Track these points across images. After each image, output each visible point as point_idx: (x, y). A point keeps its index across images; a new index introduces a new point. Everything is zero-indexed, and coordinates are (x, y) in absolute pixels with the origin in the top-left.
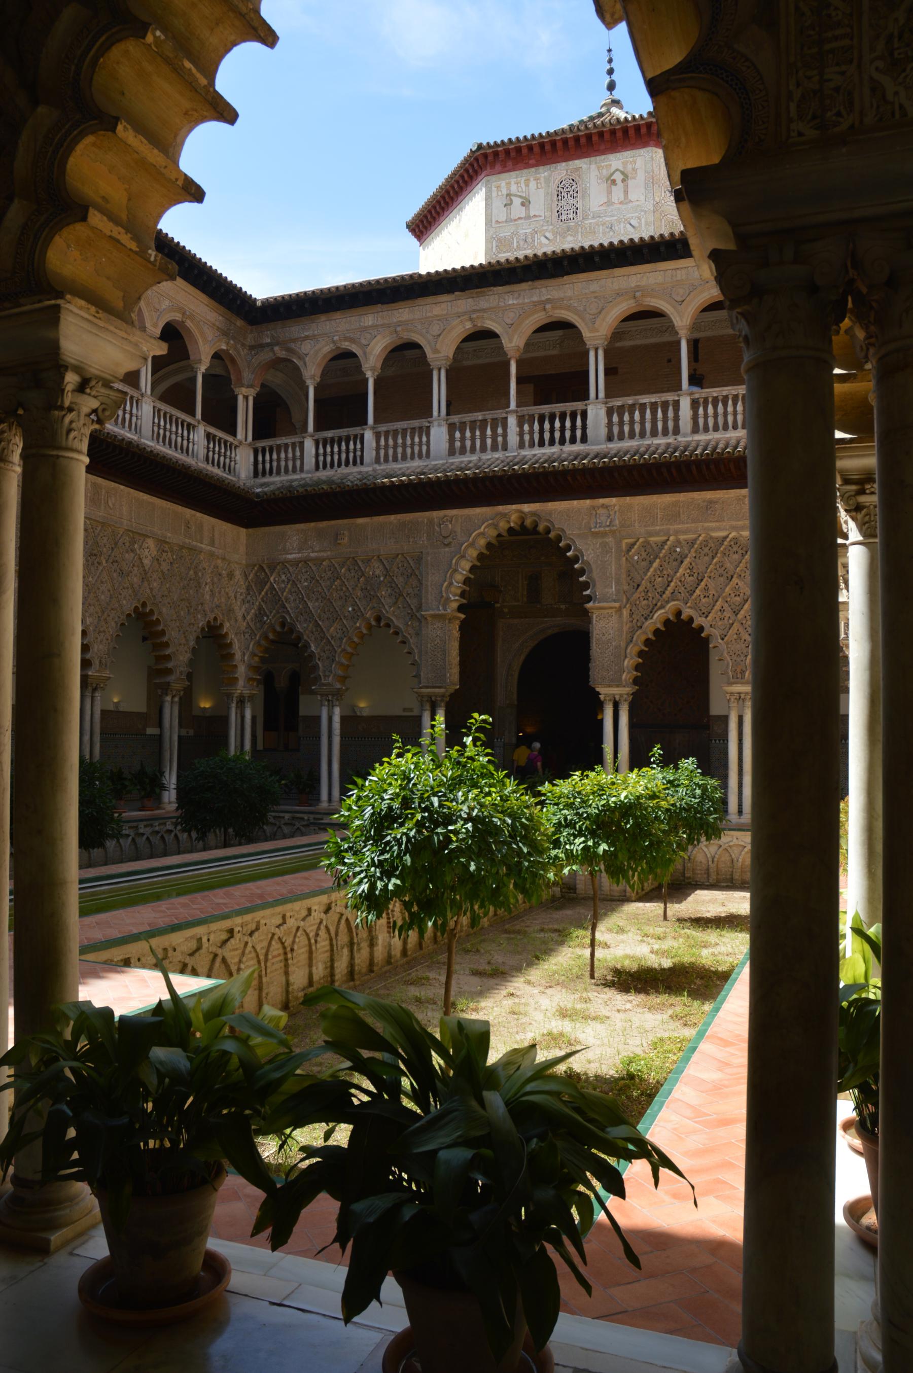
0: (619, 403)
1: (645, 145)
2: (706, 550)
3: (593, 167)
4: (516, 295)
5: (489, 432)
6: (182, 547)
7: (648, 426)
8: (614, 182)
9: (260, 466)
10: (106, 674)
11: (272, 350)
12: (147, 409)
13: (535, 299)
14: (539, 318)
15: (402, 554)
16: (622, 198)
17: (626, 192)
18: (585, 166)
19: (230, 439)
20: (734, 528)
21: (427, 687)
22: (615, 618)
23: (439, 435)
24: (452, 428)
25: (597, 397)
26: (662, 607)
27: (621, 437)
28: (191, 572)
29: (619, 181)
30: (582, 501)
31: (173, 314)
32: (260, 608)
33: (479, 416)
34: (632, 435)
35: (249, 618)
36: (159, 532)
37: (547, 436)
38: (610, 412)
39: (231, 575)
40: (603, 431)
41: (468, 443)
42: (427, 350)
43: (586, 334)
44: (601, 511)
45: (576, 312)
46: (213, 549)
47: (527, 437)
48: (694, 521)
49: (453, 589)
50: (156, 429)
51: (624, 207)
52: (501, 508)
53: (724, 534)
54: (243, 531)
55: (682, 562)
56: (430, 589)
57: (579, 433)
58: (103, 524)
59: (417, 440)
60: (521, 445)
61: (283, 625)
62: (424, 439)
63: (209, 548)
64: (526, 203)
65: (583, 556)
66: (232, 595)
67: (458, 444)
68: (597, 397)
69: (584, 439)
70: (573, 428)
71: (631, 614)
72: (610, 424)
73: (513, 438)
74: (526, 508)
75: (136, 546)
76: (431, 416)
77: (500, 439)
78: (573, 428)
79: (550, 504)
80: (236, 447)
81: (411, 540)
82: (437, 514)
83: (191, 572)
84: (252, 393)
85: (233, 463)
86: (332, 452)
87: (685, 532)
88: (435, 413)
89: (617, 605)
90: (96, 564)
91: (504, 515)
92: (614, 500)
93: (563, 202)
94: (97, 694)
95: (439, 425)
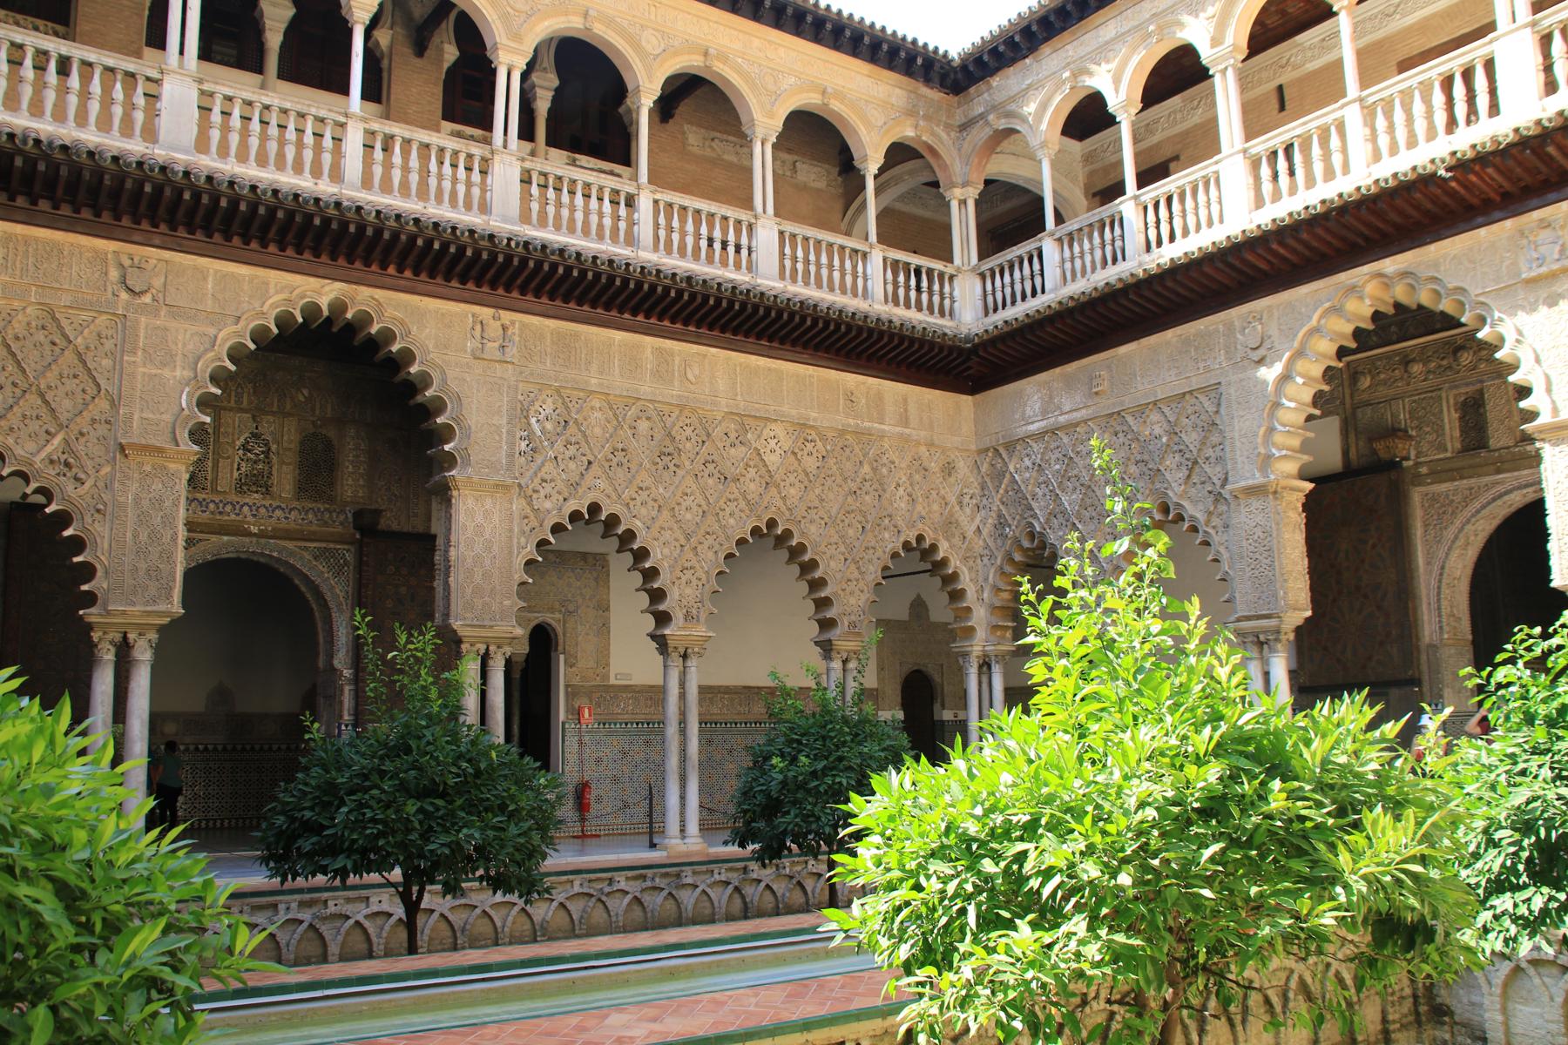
6: (842, 433)
9: (990, 299)
10: (700, 630)
11: (987, 123)
12: (767, 235)
15: (1191, 392)
19: (937, 265)
21: (1248, 618)
28: (866, 468)
31: (805, 95)
32: (1000, 516)
35: (985, 532)
36: (794, 412)
39: (949, 469)
46: (907, 431)
49: (1278, 438)
50: (788, 263)
54: (966, 400)
56: (1238, 444)
58: (682, 408)
61: (1032, 535)
63: (898, 429)
66: (953, 500)
75: (749, 436)
80: (951, 278)
82: (1235, 314)
83: (866, 468)
84: (972, 193)
85: (947, 302)
86: (1082, 253)
90: (672, 468)
91: (1352, 289)
94: (689, 663)
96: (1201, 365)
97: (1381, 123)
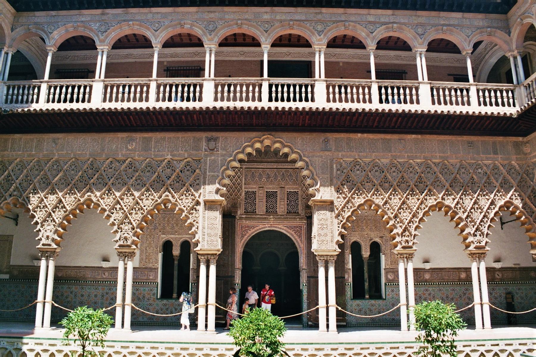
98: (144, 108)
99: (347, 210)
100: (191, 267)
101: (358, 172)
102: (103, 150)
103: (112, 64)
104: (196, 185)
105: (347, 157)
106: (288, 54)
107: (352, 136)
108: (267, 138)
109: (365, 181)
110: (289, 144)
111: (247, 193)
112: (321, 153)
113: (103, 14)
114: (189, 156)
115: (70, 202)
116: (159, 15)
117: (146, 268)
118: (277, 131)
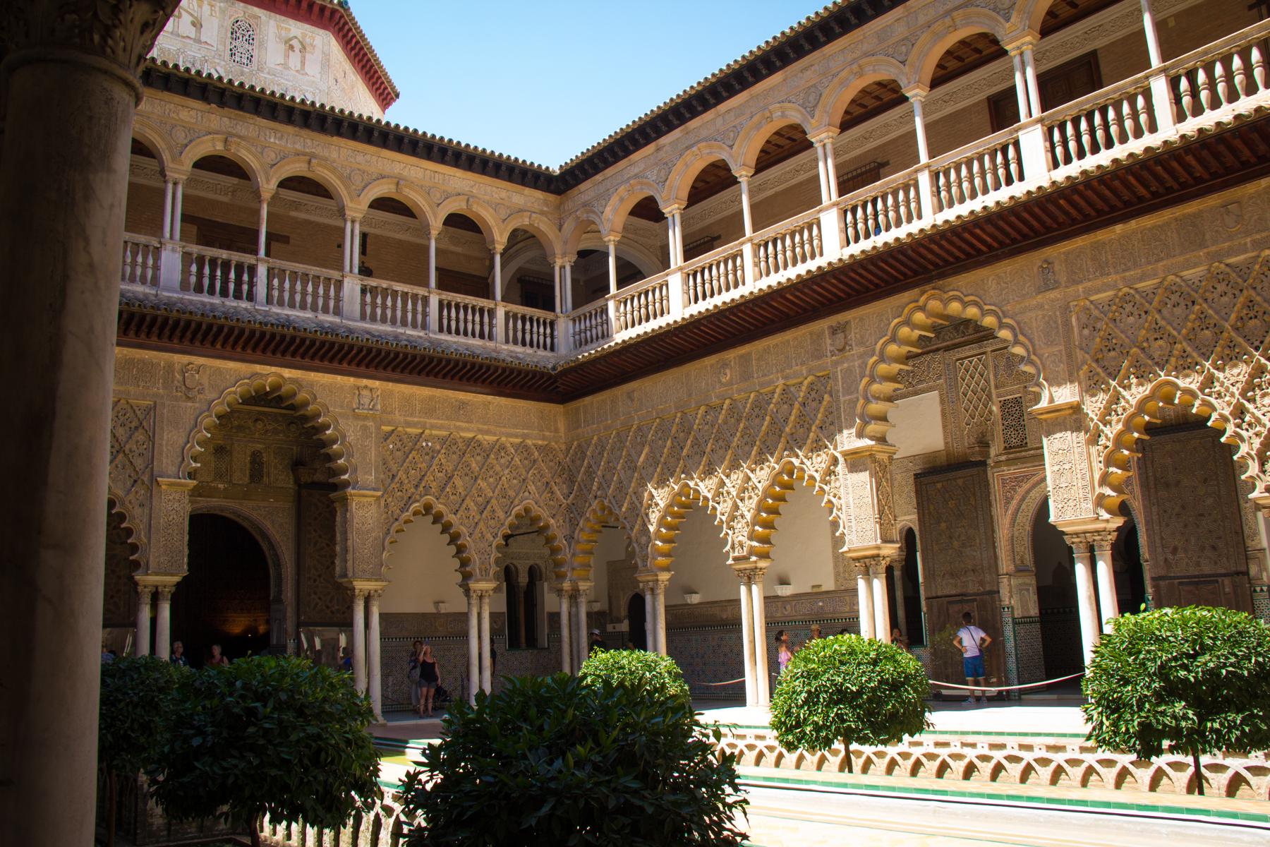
0: (374, 284)
1: (325, 27)
2: (454, 448)
3: (272, 22)
4: (279, 135)
5: (232, 275)
7: (399, 314)
8: (292, 47)
13: (299, 147)
14: (296, 168)
16: (299, 67)
17: (303, 63)
18: (263, 18)
20: (480, 431)
21: (157, 574)
22: (374, 509)
23: (171, 261)
24: (186, 257)
25: (351, 271)
26: (417, 501)
27: (373, 319)
29: (297, 50)
30: (346, 378)
33: (224, 254)
34: (384, 320)
37: (298, 298)
38: (364, 291)
40: (358, 308)
41: (206, 282)
42: (166, 156)
43: (347, 202)
44: (365, 392)
45: (341, 177)
47: (276, 293)
48: (448, 418)
51: (300, 77)
52: (258, 368)
53: (470, 435)
55: (433, 457)
57: (332, 303)
59: (140, 259)
60: (269, 300)
62: (150, 262)
64: (197, 24)
65: (344, 437)
67: (193, 279)
68: (351, 271)
69: (338, 312)
70: (326, 297)
71: (387, 505)
72: (363, 304)
73: (261, 290)
74: (287, 373)
76: (162, 236)
77: (245, 287)
78: (326, 297)
79: (312, 374)
81: (142, 384)
82: (180, 359)
87: (440, 428)
88: (167, 235)
89: (379, 493)
92: (377, 383)
93: (237, 43)
95: (173, 250)
96: (142, 384)
97: (276, 282)
98: (711, 307)
99: (1114, 418)
100: (921, 580)
101: (1131, 319)
102: (690, 395)
103: (761, 202)
104: (830, 429)
105: (1099, 291)
106: (947, 97)
107: (1101, 235)
108: (932, 297)
109: (1151, 339)
110: (972, 298)
111: (1004, 405)
112: (1040, 298)
113: (658, 150)
114: (810, 372)
115: (762, 477)
116: (732, 114)
117: (846, 590)
118: (943, 276)
